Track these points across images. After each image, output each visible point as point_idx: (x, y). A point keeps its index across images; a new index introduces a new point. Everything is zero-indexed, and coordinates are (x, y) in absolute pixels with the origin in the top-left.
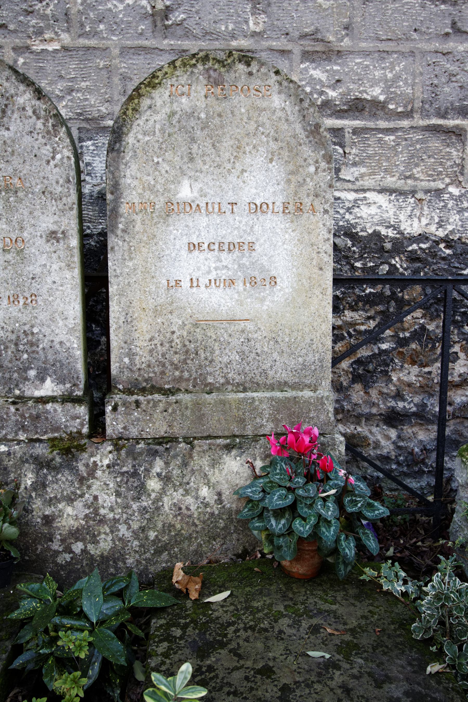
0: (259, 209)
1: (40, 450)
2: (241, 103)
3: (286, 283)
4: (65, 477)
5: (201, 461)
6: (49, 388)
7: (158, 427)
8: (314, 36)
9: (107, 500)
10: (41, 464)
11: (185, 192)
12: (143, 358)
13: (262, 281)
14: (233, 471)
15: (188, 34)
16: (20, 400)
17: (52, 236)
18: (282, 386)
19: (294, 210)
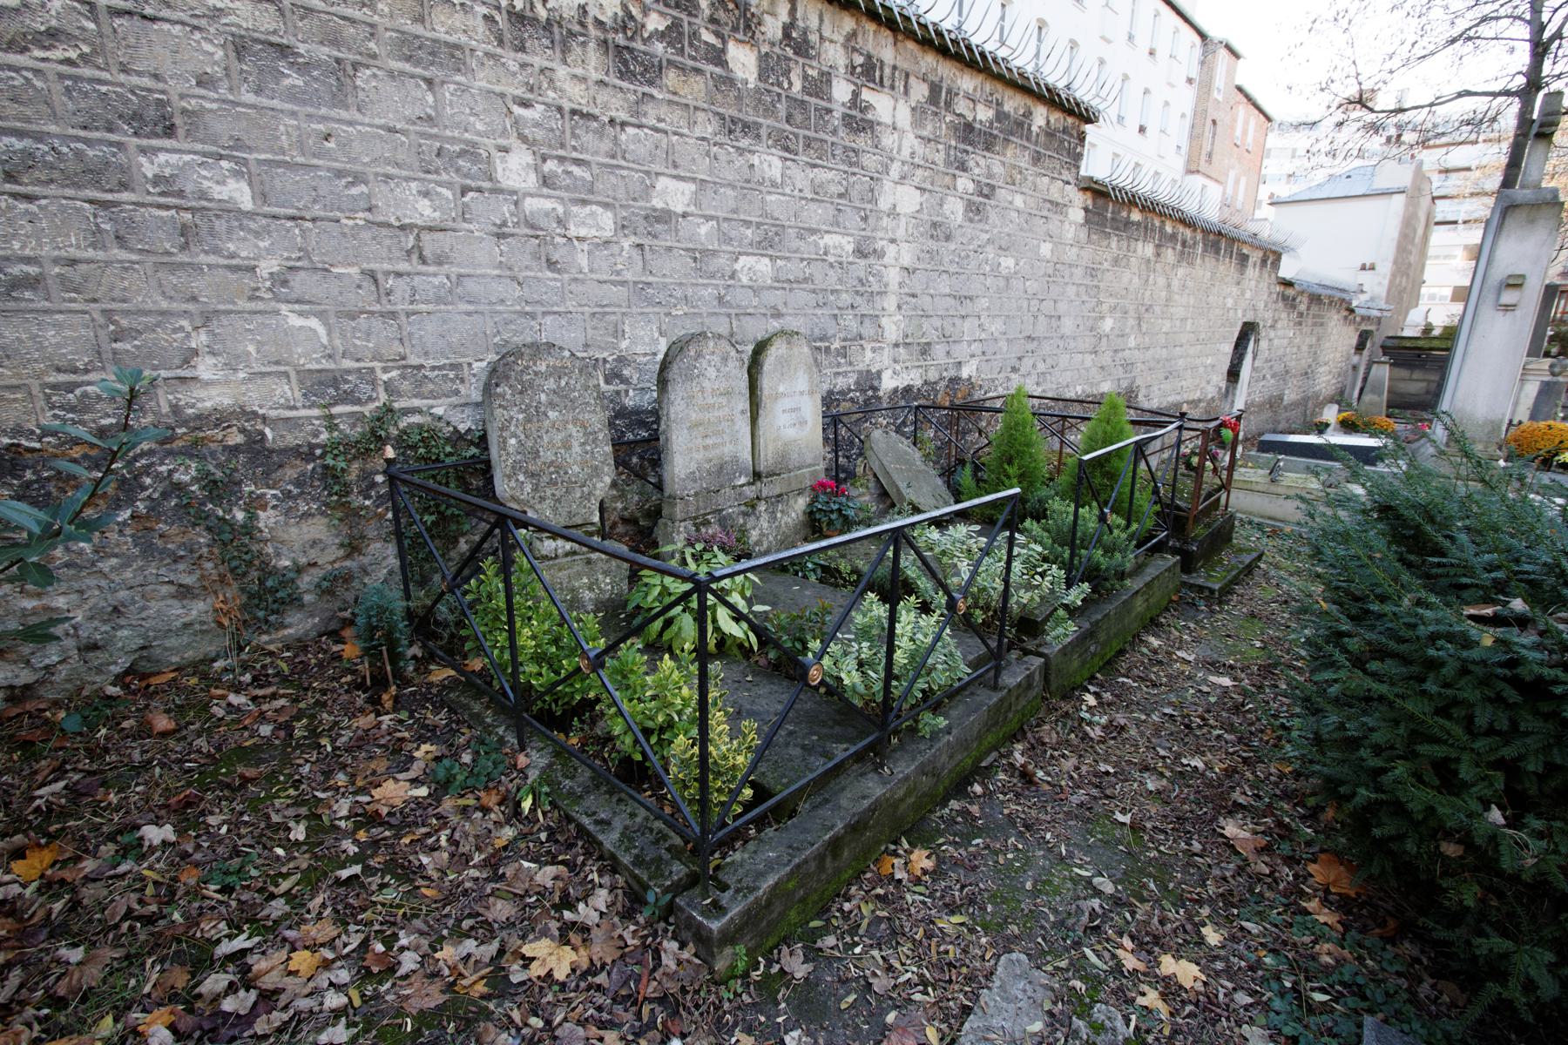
0: (802, 393)
1: (743, 508)
2: (796, 350)
3: (810, 423)
4: (752, 518)
5: (792, 502)
6: (743, 480)
7: (777, 491)
8: (774, 307)
9: (766, 525)
10: (745, 514)
11: (781, 389)
12: (771, 461)
13: (803, 423)
14: (801, 503)
15: (731, 307)
16: (734, 487)
17: (743, 412)
18: (810, 466)
19: (811, 393)
